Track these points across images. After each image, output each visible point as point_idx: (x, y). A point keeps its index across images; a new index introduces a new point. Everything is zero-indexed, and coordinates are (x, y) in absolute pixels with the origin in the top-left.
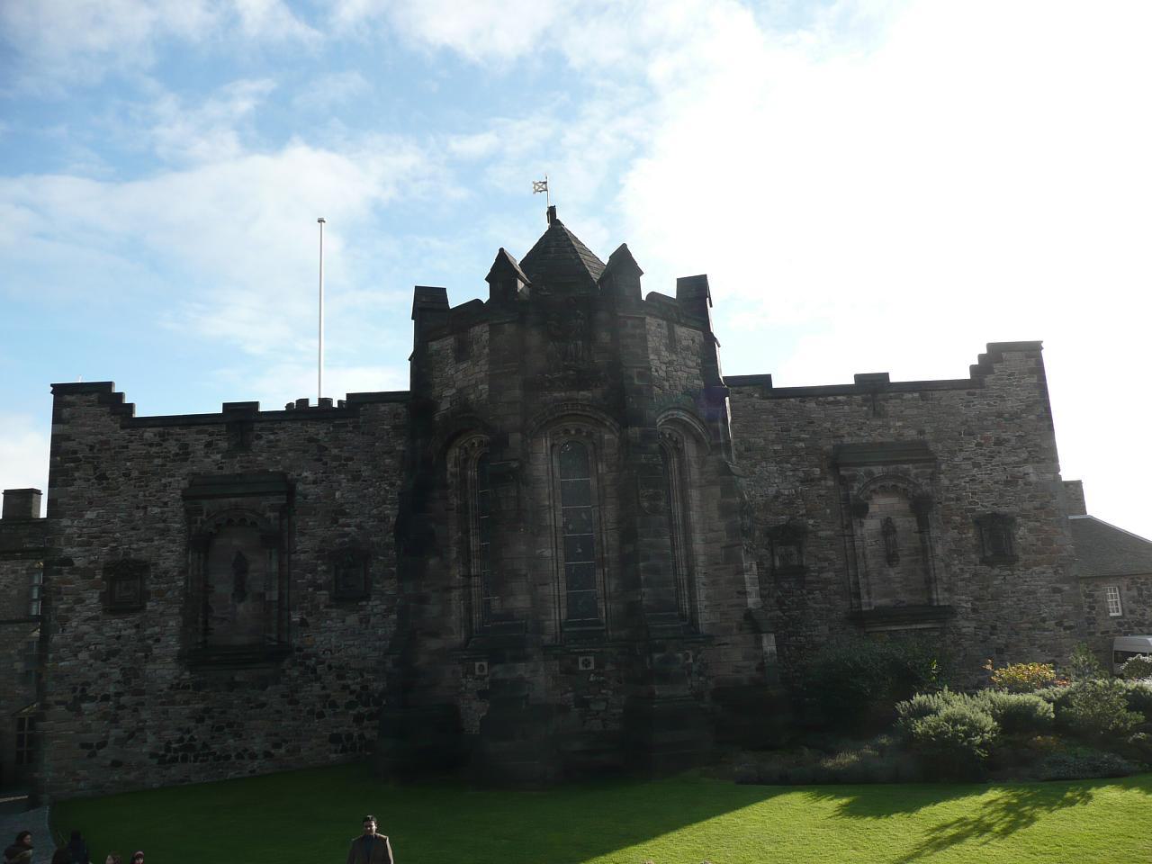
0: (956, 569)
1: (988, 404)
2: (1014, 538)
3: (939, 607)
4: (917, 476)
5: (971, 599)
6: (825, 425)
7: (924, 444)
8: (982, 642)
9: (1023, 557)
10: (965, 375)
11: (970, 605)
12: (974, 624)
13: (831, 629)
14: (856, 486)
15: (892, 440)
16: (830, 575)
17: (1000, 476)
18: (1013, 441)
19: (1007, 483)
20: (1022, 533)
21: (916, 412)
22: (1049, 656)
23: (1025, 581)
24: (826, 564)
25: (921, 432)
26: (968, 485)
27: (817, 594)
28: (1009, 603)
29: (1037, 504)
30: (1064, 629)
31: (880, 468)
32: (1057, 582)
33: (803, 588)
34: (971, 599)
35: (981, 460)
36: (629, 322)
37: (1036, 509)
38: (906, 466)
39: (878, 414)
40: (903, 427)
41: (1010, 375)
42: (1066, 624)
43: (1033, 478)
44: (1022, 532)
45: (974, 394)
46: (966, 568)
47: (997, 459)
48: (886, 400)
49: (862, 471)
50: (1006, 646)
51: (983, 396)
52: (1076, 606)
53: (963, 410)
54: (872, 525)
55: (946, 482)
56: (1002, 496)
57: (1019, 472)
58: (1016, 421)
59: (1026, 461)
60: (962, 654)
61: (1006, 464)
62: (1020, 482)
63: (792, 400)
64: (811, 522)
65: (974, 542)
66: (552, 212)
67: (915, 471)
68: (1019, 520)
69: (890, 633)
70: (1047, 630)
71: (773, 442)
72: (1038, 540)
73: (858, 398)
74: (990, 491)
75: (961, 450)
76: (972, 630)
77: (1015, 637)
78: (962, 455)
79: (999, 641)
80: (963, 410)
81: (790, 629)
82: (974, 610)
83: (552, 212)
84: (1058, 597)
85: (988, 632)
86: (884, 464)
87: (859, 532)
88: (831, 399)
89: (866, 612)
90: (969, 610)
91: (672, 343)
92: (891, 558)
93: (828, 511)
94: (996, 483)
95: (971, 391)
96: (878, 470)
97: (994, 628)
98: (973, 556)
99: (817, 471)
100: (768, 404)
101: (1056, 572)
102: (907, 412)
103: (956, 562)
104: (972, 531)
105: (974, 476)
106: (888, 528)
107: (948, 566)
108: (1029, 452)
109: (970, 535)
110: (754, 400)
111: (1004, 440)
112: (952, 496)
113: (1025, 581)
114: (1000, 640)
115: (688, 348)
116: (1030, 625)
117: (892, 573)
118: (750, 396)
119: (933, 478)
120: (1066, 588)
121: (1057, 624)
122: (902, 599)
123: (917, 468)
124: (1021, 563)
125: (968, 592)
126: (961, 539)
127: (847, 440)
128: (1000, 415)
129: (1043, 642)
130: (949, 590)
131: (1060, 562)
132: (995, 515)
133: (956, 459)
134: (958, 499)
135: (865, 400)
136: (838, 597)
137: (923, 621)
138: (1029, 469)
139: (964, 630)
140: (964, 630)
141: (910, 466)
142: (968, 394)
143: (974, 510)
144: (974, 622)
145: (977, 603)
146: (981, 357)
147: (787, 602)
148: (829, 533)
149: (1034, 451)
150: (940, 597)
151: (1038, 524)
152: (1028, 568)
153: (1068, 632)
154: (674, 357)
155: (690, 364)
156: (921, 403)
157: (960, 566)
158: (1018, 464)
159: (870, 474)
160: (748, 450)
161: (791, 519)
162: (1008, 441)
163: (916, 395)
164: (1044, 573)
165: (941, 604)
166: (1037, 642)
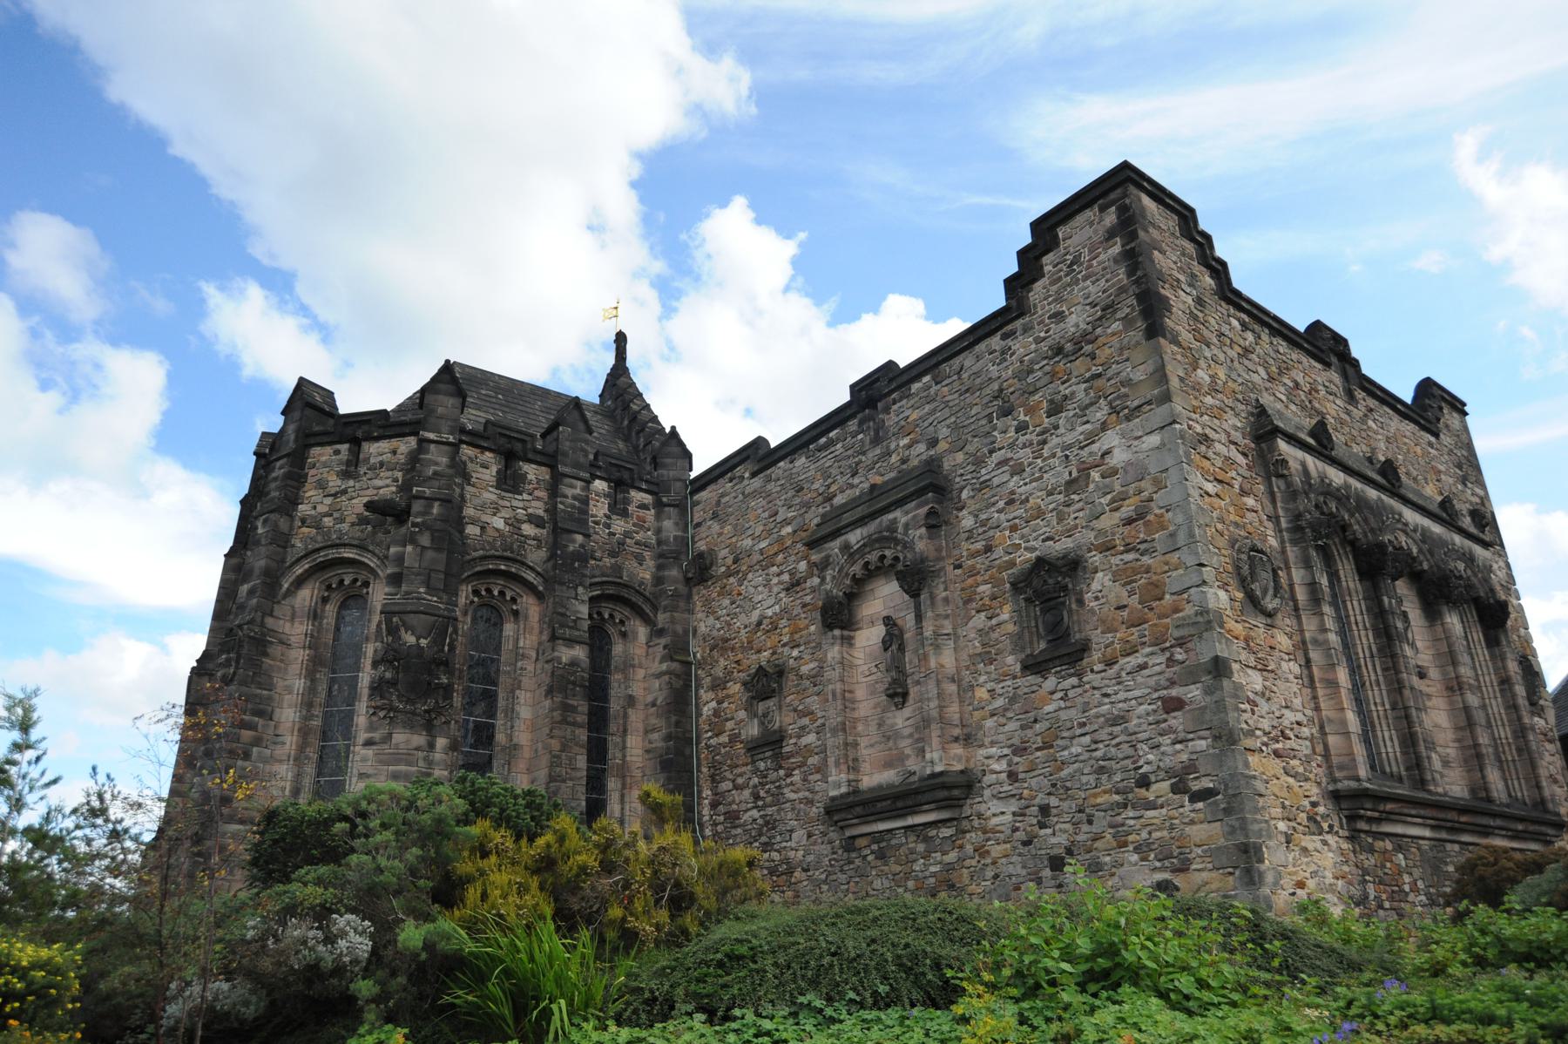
0: (982, 693)
1: (1038, 341)
2: (1081, 602)
3: (934, 775)
4: (906, 526)
5: (1006, 751)
6: (815, 486)
7: (932, 466)
8: (1026, 843)
9: (1098, 638)
10: (998, 300)
11: (1002, 766)
12: (1014, 806)
13: (810, 836)
14: (829, 573)
15: (893, 475)
16: (810, 738)
17: (1059, 474)
18: (1081, 395)
19: (1070, 483)
20: (1102, 588)
21: (927, 408)
22: (1155, 869)
23: (1106, 695)
24: (806, 721)
25: (933, 443)
26: (1002, 516)
27: (797, 777)
28: (1074, 750)
29: (1127, 510)
30: (1192, 800)
31: (858, 531)
32: (1172, 683)
33: (781, 767)
34: (1006, 751)
35: (1024, 455)
36: (278, 464)
37: (1129, 522)
38: (891, 516)
39: (876, 441)
40: (909, 446)
41: (1072, 264)
42: (1196, 786)
43: (1119, 458)
44: (1101, 581)
45: (1012, 334)
46: (998, 688)
47: (1054, 441)
48: (887, 410)
49: (834, 546)
50: (1070, 852)
51: (1026, 329)
52: (1216, 738)
53: (994, 370)
54: (869, 637)
55: (968, 522)
56: (1060, 520)
57: (1091, 454)
58: (1088, 348)
59: (1104, 427)
60: (989, 873)
61: (1069, 447)
62: (1095, 475)
63: (781, 464)
64: (795, 653)
65: (1011, 628)
66: (621, 339)
67: (904, 520)
68: (1095, 558)
69: (877, 837)
70: (1152, 806)
71: (759, 538)
72: (1131, 593)
73: (853, 425)
74: (1040, 514)
75: (991, 452)
76: (1008, 818)
77: (1085, 828)
78: (997, 457)
79: (1054, 840)
80: (994, 370)
81: (764, 839)
82: (1012, 776)
83: (621, 339)
84: (1177, 721)
85: (1035, 821)
86: (861, 522)
87: (830, 655)
88: (823, 440)
89: (833, 799)
90: (1004, 775)
91: (350, 470)
92: (898, 694)
93: (813, 628)
94: (1050, 494)
95: (1009, 327)
96: (855, 537)
97: (1045, 810)
98: (1010, 659)
99: (803, 566)
100: (757, 483)
101: (1171, 661)
102: (914, 416)
103: (982, 679)
104: (1007, 608)
105: (1013, 493)
106: (893, 637)
107: (966, 690)
108: (1110, 403)
109: (1005, 616)
110: (746, 482)
111: (1066, 398)
112: (979, 546)
113: (1106, 695)
114: (1055, 839)
115: (382, 464)
116: (1117, 798)
117: (901, 720)
118: (742, 478)
119: (934, 523)
120: (1194, 693)
121: (1175, 789)
122: (913, 768)
123: (907, 513)
124: (1096, 656)
125: (1001, 738)
126: (992, 629)
127: (839, 500)
128: (1058, 350)
129: (1144, 835)
130: (968, 740)
131: (1177, 634)
132: (1040, 562)
133: (983, 471)
134: (988, 549)
135: (861, 423)
136: (818, 776)
137: (913, 810)
138: (1111, 439)
139: (995, 821)
140: (995, 821)
141: (897, 514)
142: (1005, 337)
143: (1012, 564)
144: (1013, 800)
145: (1016, 759)
146: (1022, 254)
147: (762, 793)
148: (812, 665)
149: (1118, 397)
150: (936, 756)
151: (1130, 556)
152: (1110, 663)
153: (1200, 805)
154: (351, 483)
155: (378, 483)
156: (934, 388)
157: (990, 685)
158: (1091, 438)
159: (846, 547)
160: (736, 561)
161: (774, 653)
162: (1073, 393)
163: (926, 379)
164: (1143, 667)
165: (938, 769)
166: (1131, 838)
